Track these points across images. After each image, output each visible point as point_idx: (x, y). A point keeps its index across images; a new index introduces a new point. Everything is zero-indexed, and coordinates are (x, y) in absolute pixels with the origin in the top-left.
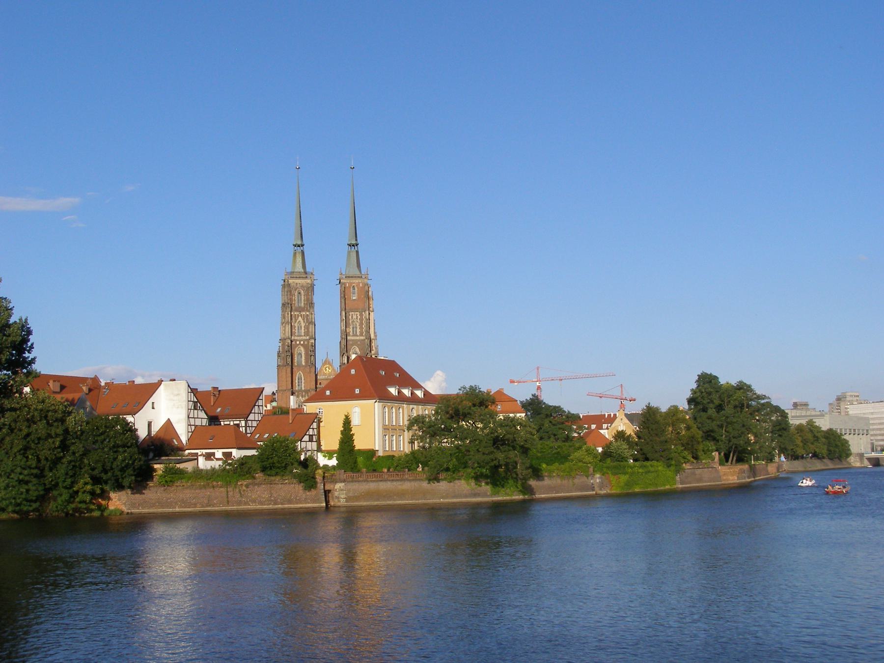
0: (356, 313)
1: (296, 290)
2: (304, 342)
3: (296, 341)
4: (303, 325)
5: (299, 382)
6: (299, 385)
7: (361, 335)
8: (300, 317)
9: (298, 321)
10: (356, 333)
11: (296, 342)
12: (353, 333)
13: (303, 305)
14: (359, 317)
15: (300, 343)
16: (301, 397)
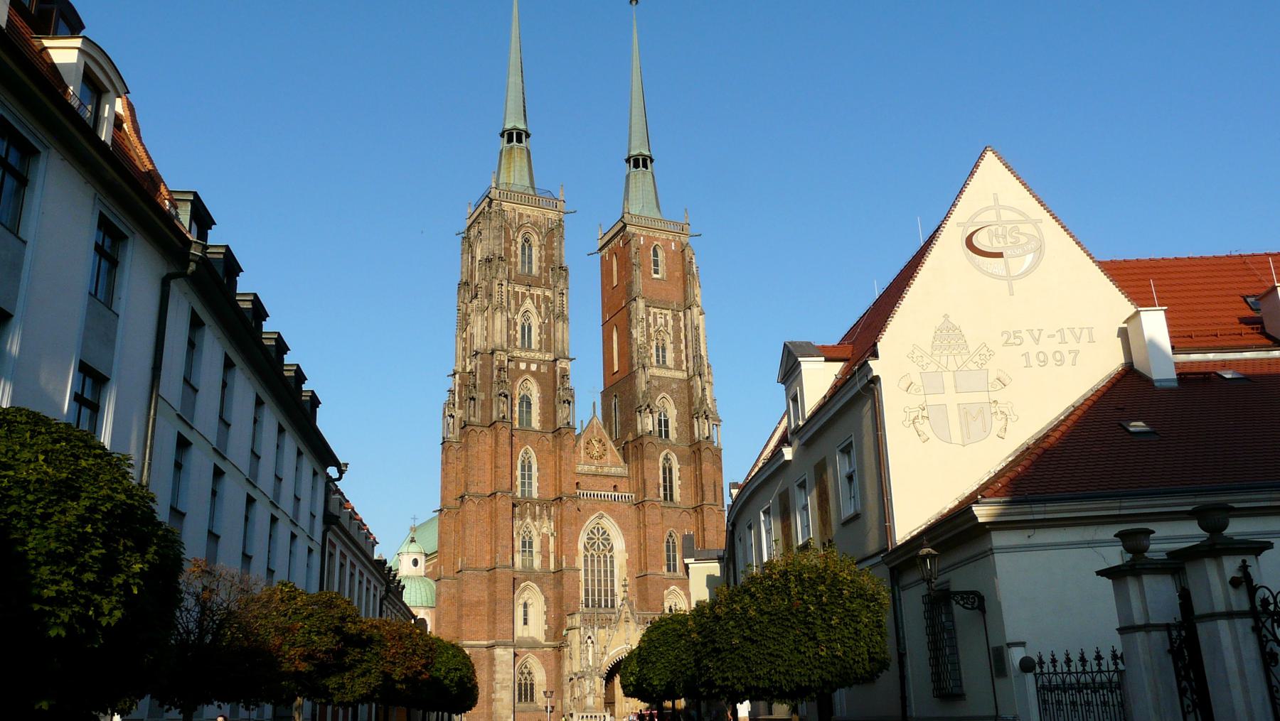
0: (665, 312)
1: (519, 229)
2: (538, 367)
3: (520, 359)
5: (523, 476)
6: (523, 484)
7: (678, 366)
8: (528, 301)
9: (522, 309)
10: (664, 362)
11: (517, 366)
12: (658, 361)
13: (535, 270)
14: (671, 323)
15: (528, 366)
16: (529, 520)
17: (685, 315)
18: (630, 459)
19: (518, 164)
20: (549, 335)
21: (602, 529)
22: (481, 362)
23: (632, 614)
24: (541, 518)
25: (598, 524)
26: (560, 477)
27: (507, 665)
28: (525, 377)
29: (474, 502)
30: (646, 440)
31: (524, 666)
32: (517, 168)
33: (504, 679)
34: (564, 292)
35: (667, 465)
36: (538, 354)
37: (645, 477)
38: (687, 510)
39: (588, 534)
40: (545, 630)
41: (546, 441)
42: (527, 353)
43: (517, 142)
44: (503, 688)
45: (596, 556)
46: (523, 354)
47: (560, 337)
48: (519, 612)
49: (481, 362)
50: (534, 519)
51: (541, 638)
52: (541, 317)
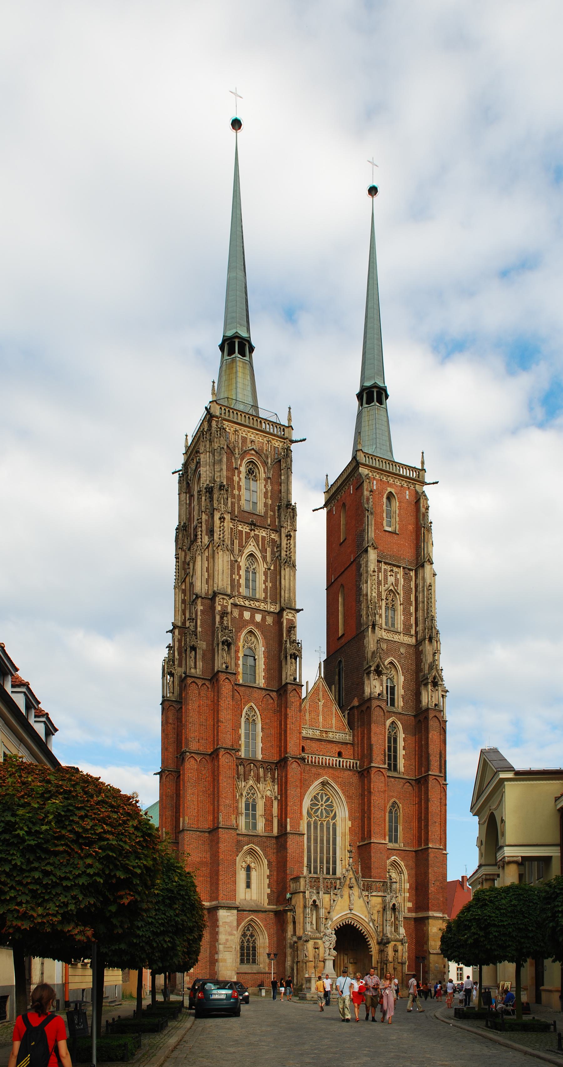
2: (264, 619)
4: (261, 567)
5: (247, 736)
6: (247, 745)
8: (252, 542)
11: (241, 615)
15: (252, 617)
18: (356, 724)
19: (239, 380)
20: (274, 581)
24: (265, 780)
26: (286, 737)
28: (249, 628)
31: (246, 929)
32: (240, 385)
34: (292, 534)
36: (263, 604)
37: (373, 742)
41: (270, 699)
42: (252, 602)
43: (239, 353)
46: (247, 603)
47: (287, 586)
48: (241, 876)
50: (258, 780)
51: (265, 903)
52: (267, 563)
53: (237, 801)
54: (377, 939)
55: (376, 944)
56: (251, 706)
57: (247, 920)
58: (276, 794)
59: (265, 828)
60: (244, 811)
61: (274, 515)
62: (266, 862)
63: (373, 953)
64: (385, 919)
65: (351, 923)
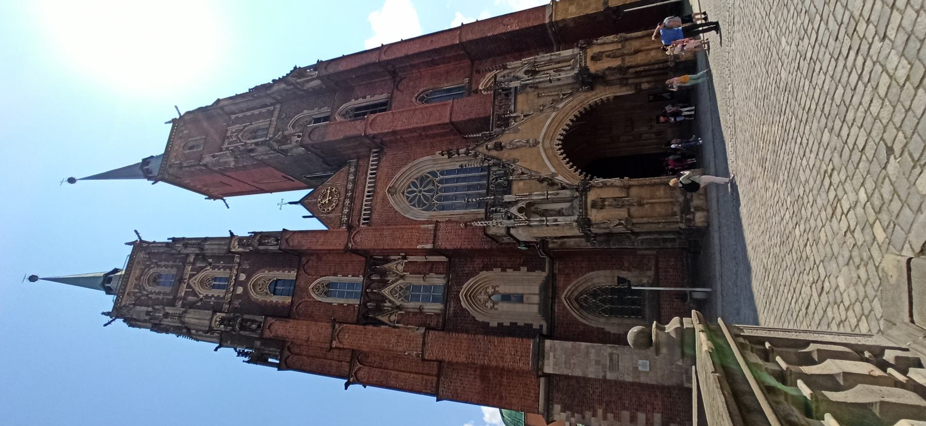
0: (229, 134)
5: (341, 295)
11: (239, 296)
17: (234, 113)
21: (409, 187)
22: (229, 342)
23: (490, 138)
25: (403, 193)
27: (573, 354)
29: (359, 369)
30: (307, 141)
33: (597, 363)
35: (351, 114)
38: (396, 84)
39: (414, 205)
40: (528, 271)
44: (614, 366)
45: (440, 194)
49: (229, 342)
51: (540, 276)
52: (206, 267)
53: (408, 313)
54: (585, 91)
55: (593, 93)
56: (313, 288)
57: (568, 307)
58: (400, 257)
59: (440, 274)
60: (418, 304)
61: (179, 258)
62: (484, 274)
63: (611, 95)
64: (550, 85)
65: (559, 140)
